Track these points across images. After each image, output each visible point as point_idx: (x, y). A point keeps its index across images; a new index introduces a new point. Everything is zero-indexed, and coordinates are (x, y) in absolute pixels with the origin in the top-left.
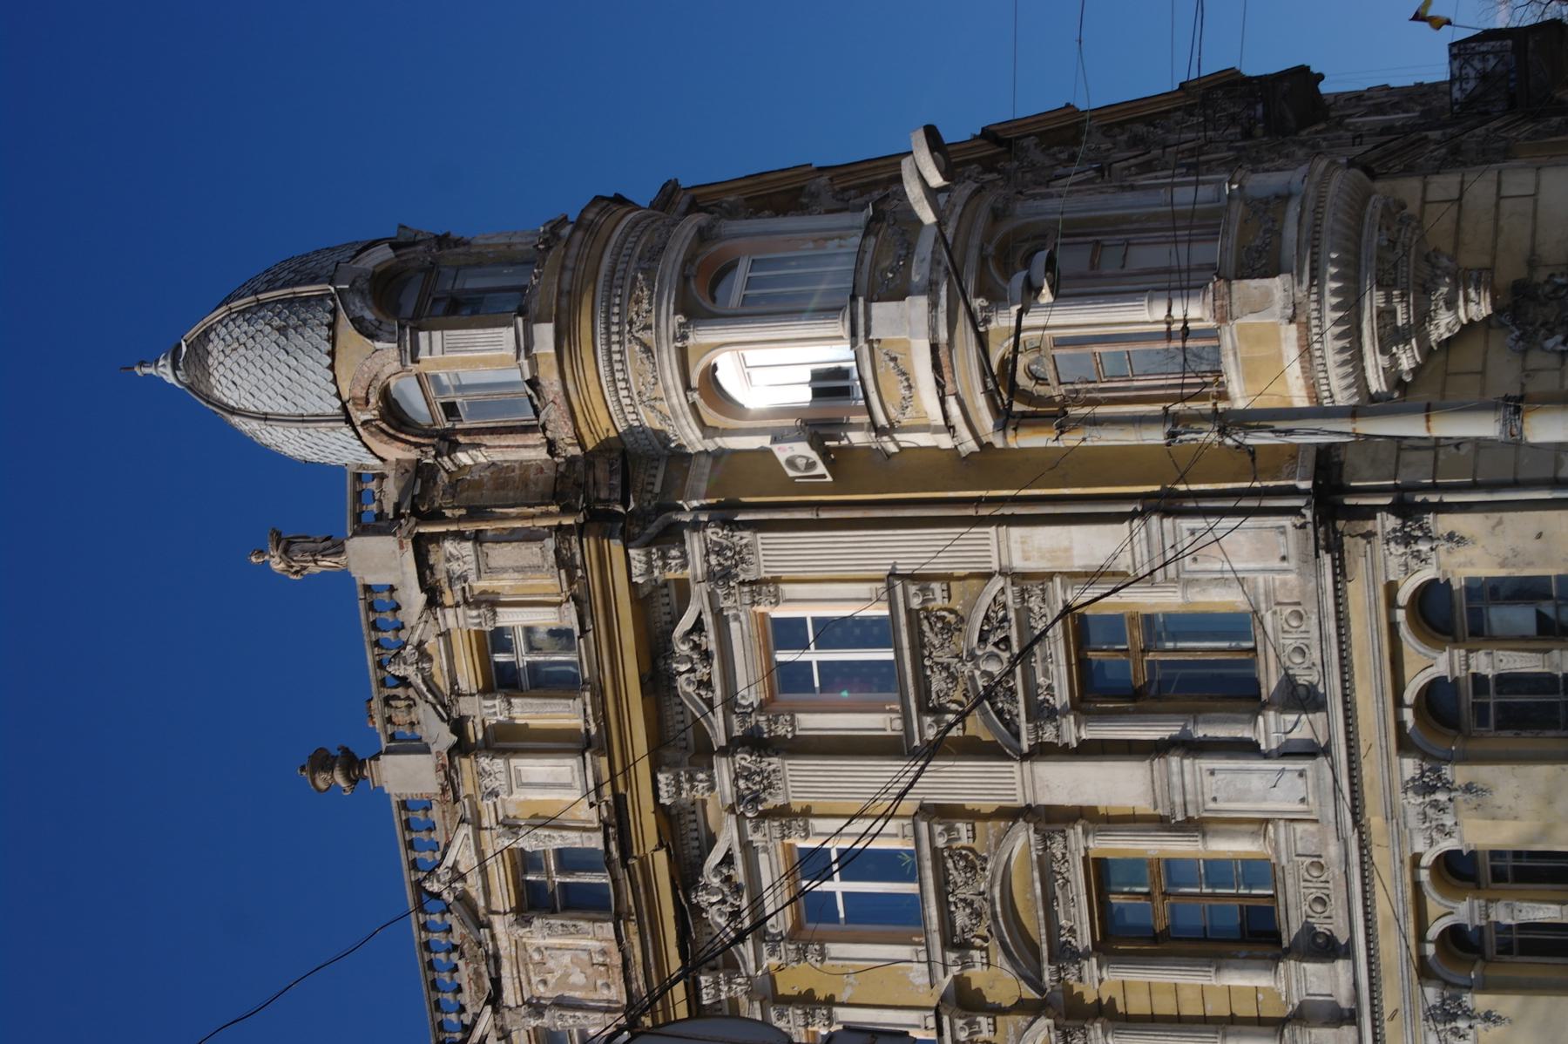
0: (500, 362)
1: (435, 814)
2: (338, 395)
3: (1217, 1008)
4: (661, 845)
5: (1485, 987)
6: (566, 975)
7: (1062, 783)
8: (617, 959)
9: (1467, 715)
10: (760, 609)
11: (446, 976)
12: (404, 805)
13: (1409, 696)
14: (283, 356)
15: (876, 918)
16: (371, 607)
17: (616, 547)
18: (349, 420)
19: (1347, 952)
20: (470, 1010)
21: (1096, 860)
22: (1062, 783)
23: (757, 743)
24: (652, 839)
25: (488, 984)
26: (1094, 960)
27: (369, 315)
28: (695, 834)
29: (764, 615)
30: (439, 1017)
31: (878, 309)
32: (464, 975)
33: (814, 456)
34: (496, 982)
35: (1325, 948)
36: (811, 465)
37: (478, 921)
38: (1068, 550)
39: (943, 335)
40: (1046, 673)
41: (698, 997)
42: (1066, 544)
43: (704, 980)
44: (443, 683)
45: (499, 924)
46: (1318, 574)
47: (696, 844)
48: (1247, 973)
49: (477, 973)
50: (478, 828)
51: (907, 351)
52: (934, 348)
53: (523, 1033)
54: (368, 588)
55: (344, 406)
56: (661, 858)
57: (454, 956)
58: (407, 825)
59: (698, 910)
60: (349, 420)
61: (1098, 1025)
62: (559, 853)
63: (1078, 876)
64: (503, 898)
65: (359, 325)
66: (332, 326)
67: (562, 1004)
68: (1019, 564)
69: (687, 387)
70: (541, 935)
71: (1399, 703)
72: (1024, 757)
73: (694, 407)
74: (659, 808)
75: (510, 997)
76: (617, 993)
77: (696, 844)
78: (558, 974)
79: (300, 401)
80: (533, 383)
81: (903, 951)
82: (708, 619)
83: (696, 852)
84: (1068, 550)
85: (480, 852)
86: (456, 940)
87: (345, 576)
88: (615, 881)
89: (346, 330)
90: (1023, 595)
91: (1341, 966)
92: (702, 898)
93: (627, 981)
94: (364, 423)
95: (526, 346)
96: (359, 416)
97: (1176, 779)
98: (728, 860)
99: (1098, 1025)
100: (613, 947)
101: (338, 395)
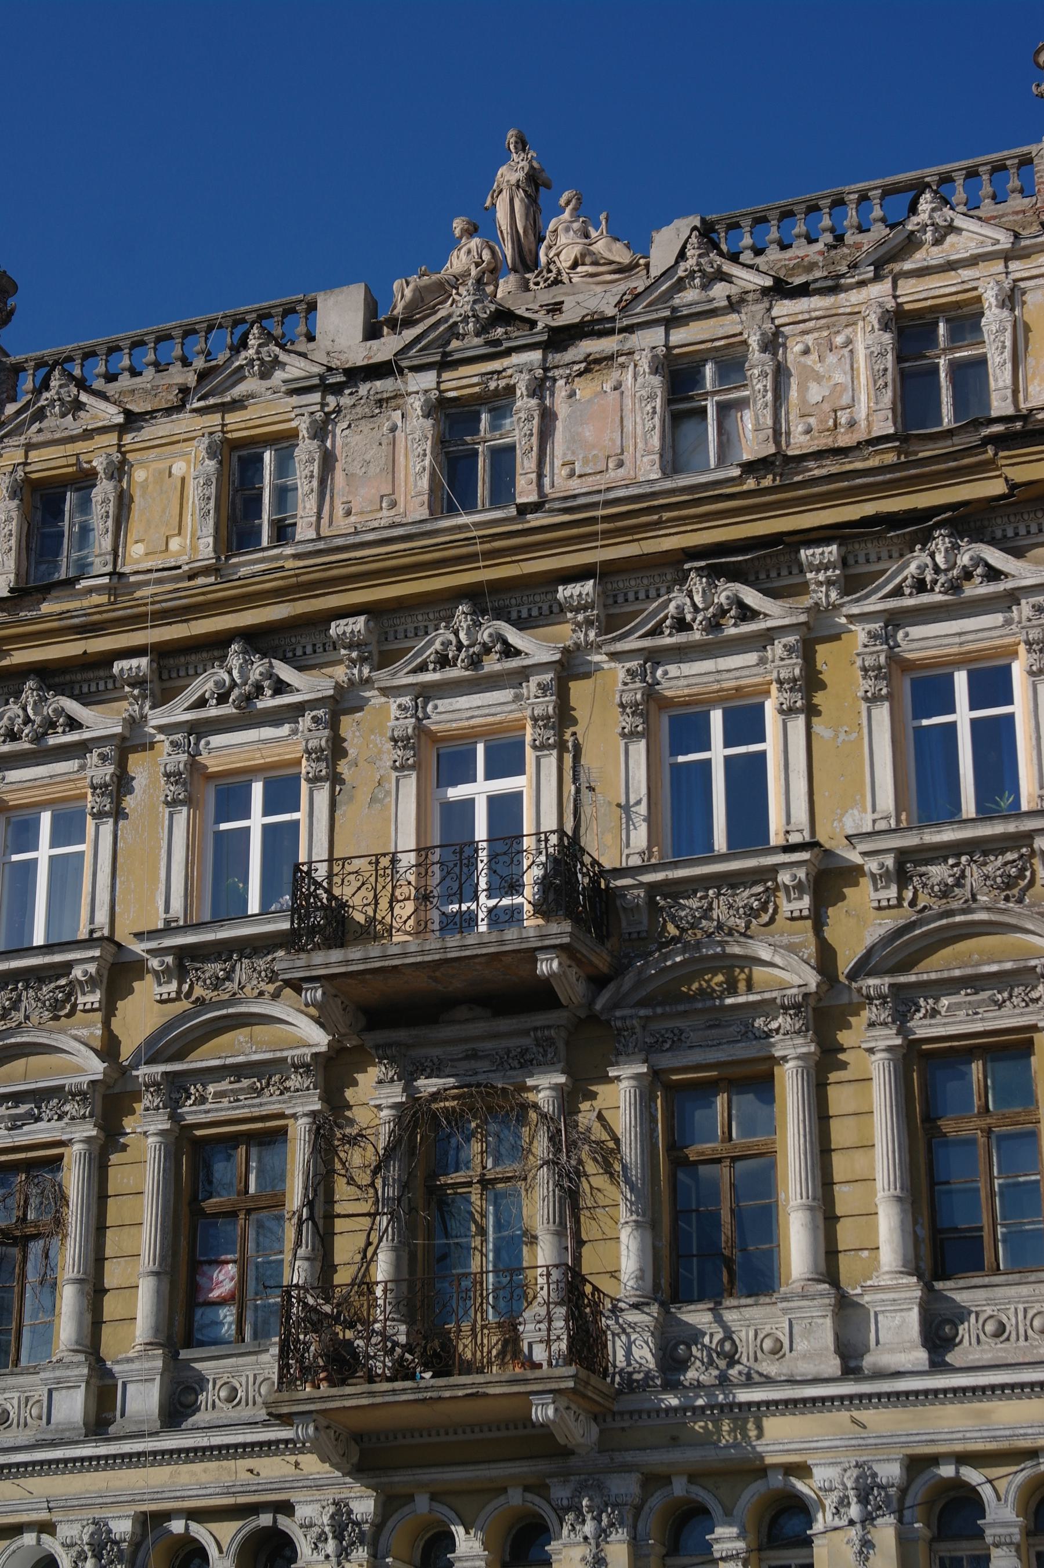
1: (1017, 202)
3: (845, 1198)
4: (1013, 486)
5: (903, 1540)
6: (818, 378)
8: (844, 440)
11: (800, 228)
12: (1026, 162)
15: (926, 765)
19: (938, 1365)
20: (759, 261)
21: (1030, 1042)
24: (1021, 474)
25: (798, 281)
26: (898, 1041)
28: (1022, 531)
30: (746, 223)
32: (801, 250)
34: (803, 291)
35: (939, 1334)
37: (882, 264)
41: (809, 544)
43: (832, 551)
45: (881, 290)
47: (1010, 533)
48: (897, 1237)
49: (811, 267)
50: (1007, 257)
53: (738, 329)
56: (996, 488)
57: (828, 238)
58: (998, 168)
59: (925, 538)
61: (812, 1048)
62: (981, 362)
63: (1008, 1018)
64: (915, 293)
67: (780, 374)
70: (868, 345)
75: (785, 308)
76: (799, 442)
77: (1010, 533)
78: (818, 367)
81: (886, 800)
83: (999, 534)
85: (973, 261)
86: (850, 238)
88: (950, 433)
91: (920, 1357)
92: (941, 544)
93: (819, 455)
98: (994, 574)
99: (812, 1048)
100: (861, 434)
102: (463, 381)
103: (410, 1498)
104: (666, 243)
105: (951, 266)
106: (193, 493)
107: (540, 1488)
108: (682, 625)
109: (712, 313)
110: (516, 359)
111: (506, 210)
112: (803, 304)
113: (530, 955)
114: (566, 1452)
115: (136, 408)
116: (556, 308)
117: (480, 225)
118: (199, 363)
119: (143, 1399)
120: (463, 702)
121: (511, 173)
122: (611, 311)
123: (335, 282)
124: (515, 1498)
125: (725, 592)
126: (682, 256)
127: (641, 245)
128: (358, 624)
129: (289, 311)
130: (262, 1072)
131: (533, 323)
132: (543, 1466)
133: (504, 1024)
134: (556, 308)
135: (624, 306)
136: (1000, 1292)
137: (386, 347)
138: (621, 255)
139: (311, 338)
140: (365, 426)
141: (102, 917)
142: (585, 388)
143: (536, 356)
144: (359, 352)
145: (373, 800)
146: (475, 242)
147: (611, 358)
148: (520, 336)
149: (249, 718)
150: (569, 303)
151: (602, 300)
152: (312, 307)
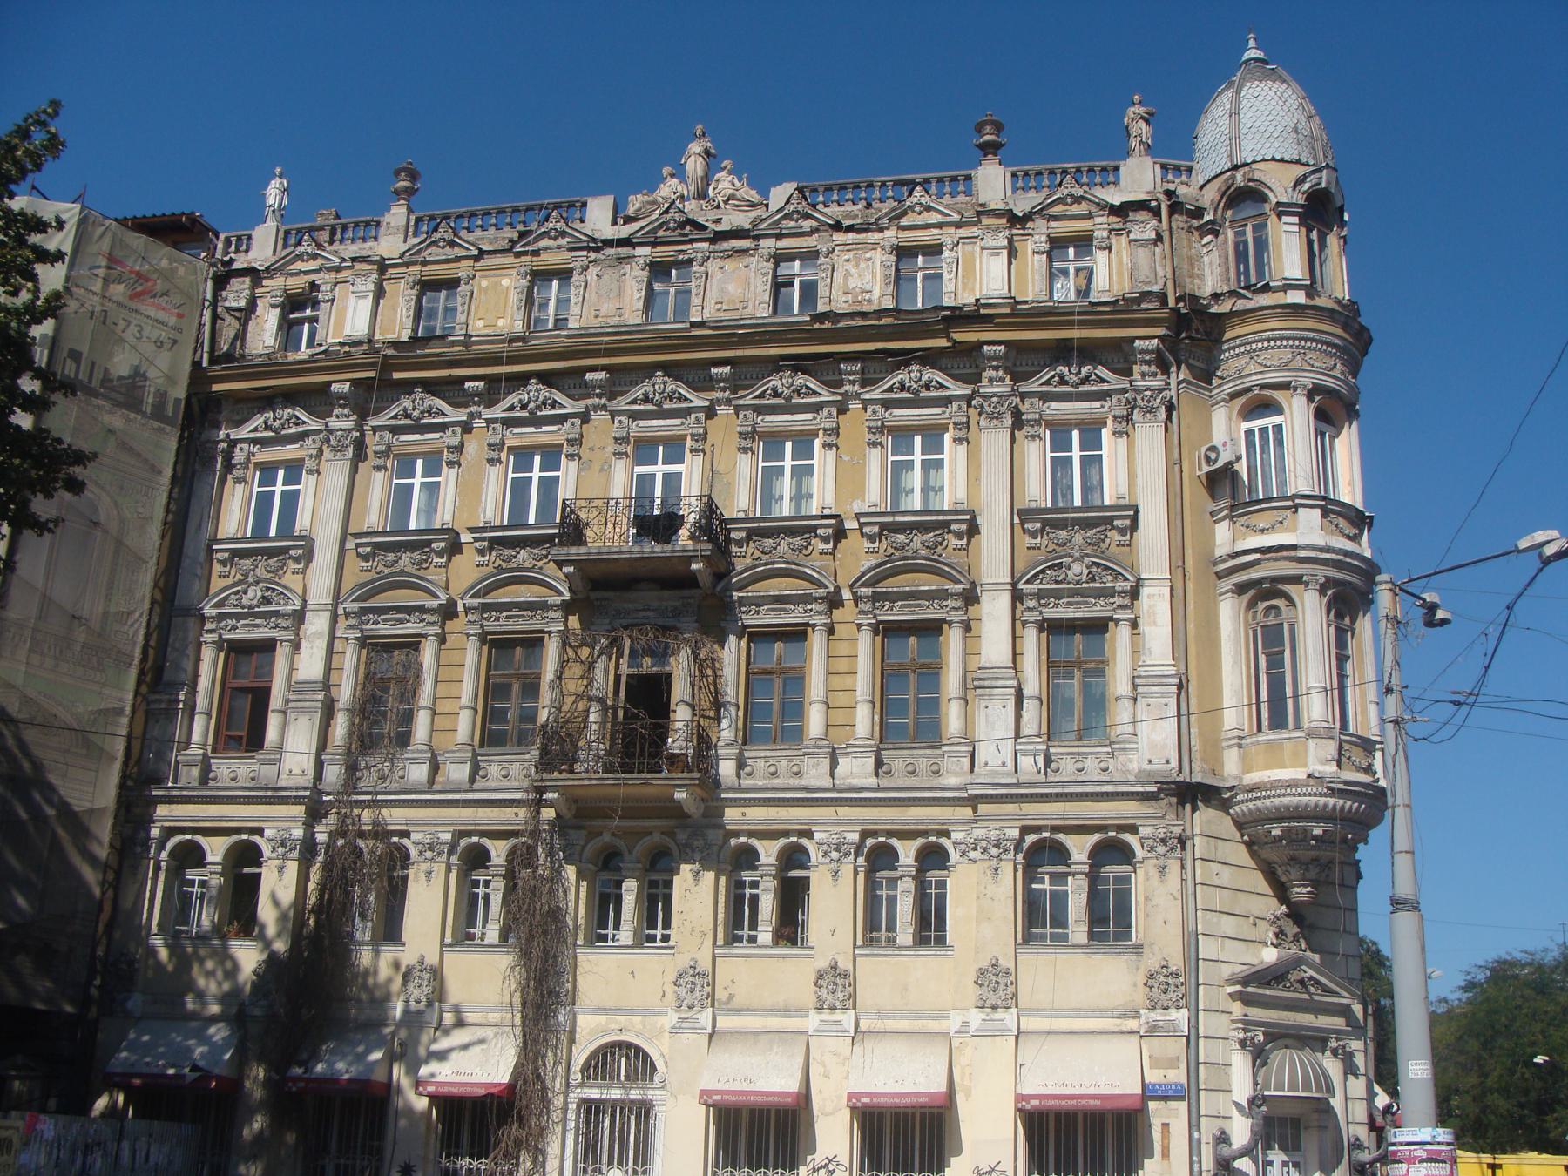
1: (962, 198)
2: (1254, 162)
4: (955, 342)
7: (995, 611)
8: (866, 308)
10: (1110, 422)
11: (849, 196)
12: (968, 178)
13: (1060, 837)
14: (1280, 128)
16: (1104, 169)
17: (1161, 331)
20: (826, 210)
24: (959, 336)
25: (847, 223)
27: (1306, 186)
29: (1105, 424)
30: (821, 189)
31: (1318, 511)
32: (849, 207)
33: (1220, 464)
34: (850, 229)
37: (895, 218)
38: (1155, 624)
39: (1302, 554)
40: (1069, 604)
42: (1159, 622)
44: (1052, 211)
46: (1143, 783)
49: (856, 217)
51: (1287, 530)
52: (1294, 548)
54: (1117, 168)
55: (1246, 164)
57: (864, 203)
58: (954, 179)
59: (907, 364)
60: (1236, 168)
65: (1299, 182)
66: (1298, 162)
68: (1145, 592)
69: (1263, 387)
71: (1055, 829)
72: (1014, 584)
73: (1249, 390)
74: (982, 344)
79: (1249, 137)
80: (1266, 288)
82: (1105, 387)
84: (1155, 624)
85: (940, 226)
86: (876, 204)
87: (1128, 154)
88: (922, 311)
89: (1300, 171)
90: (1122, 593)
92: (915, 368)
93: (852, 315)
94: (1233, 177)
96: (1239, 176)
97: (1000, 683)
100: (875, 307)
101: (1254, 162)
102: (664, 253)
103: (600, 834)
104: (780, 194)
105: (926, 227)
107: (670, 833)
108: (776, 394)
109: (802, 234)
110: (695, 245)
111: (694, 165)
112: (851, 235)
113: (690, 559)
114: (687, 816)
115: (485, 248)
116: (718, 221)
117: (680, 174)
118: (521, 228)
120: (655, 422)
122: (748, 227)
123: (596, 193)
124: (657, 838)
125: (800, 380)
126: (788, 202)
127: (765, 193)
128: (602, 375)
129: (571, 205)
131: (706, 228)
132: (672, 823)
133: (666, 593)
134: (718, 221)
135: (754, 226)
136: (915, 752)
137: (624, 231)
138: (753, 196)
139: (582, 221)
140: (610, 271)
142: (729, 265)
143: (705, 245)
144: (609, 232)
145: (602, 470)
146: (675, 181)
147: (747, 250)
149: (536, 421)
150: (725, 219)
151: (742, 219)
152: (584, 205)
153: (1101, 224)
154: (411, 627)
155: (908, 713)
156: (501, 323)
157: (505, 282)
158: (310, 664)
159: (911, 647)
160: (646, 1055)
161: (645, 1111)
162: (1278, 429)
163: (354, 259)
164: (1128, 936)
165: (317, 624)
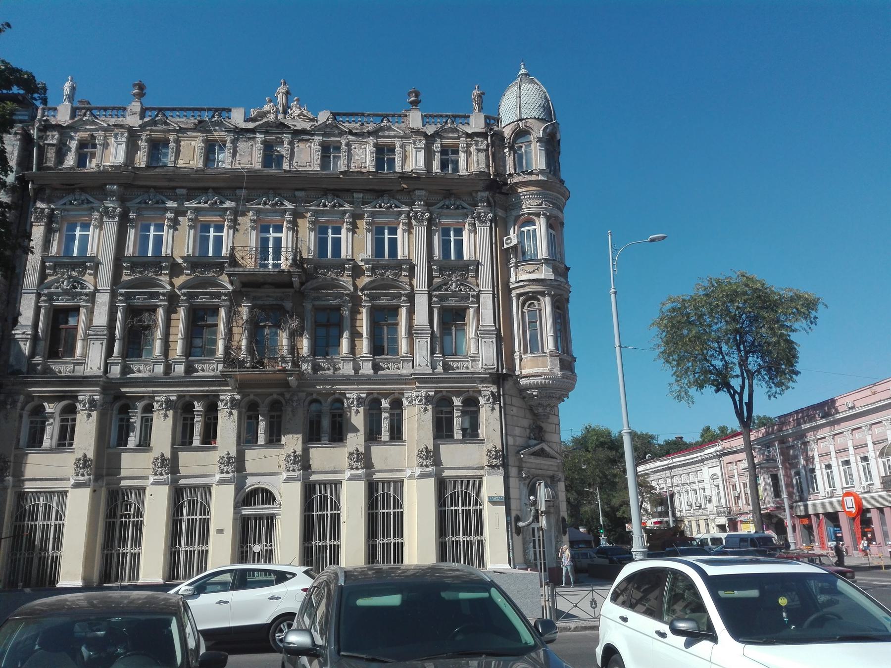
0: (537, 165)
9: (440, 409)
15: (378, 244)
18: (521, 120)
22: (421, 302)
23: (430, 221)
32: (353, 125)
36: (507, 244)
59: (382, 196)
60: (521, 120)
64: (381, 141)
68: (482, 296)
69: (529, 214)
70: (370, 148)
76: (353, 169)
80: (531, 173)
81: (370, 253)
85: (394, 137)
87: (472, 112)
95: (541, 172)
105: (389, 137)
106: (197, 151)
107: (282, 395)
114: (290, 387)
118: (199, 118)
119: (180, 369)
121: (282, 89)
123: (237, 106)
124: (275, 396)
130: (218, 295)
132: (283, 390)
137: (251, 125)
141: (169, 251)
144: (243, 125)
148: (285, 130)
151: (307, 126)
152: (230, 110)
153: (462, 142)
154: (154, 302)
155: (380, 347)
156: (191, 162)
157: (193, 143)
158: (101, 318)
159: (382, 319)
160: (271, 493)
161: (271, 518)
162: (534, 231)
163: (115, 125)
164: (477, 436)
165: (103, 299)
